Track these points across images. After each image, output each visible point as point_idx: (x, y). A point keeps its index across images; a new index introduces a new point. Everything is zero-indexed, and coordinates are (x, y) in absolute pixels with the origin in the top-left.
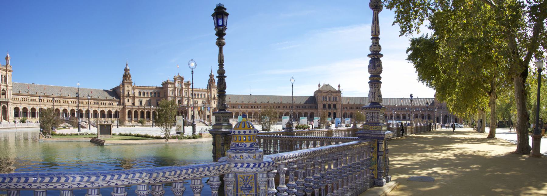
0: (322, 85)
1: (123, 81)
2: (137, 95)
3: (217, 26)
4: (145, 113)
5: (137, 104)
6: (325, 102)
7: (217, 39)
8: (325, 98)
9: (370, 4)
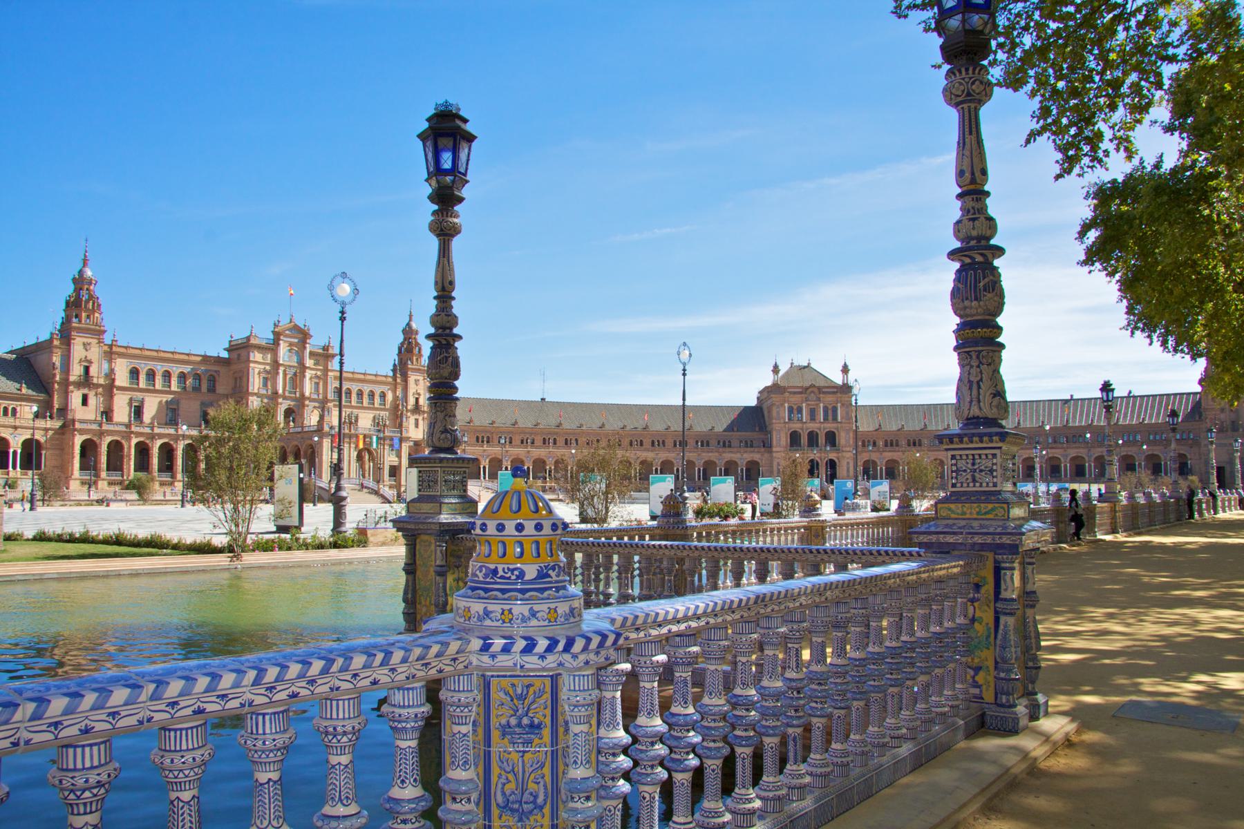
0: (783, 369)
1: (66, 323)
2: (122, 379)
3: (436, 171)
4: (155, 451)
5: (121, 413)
6: (796, 426)
7: (434, 213)
8: (795, 411)
9: (945, 90)
